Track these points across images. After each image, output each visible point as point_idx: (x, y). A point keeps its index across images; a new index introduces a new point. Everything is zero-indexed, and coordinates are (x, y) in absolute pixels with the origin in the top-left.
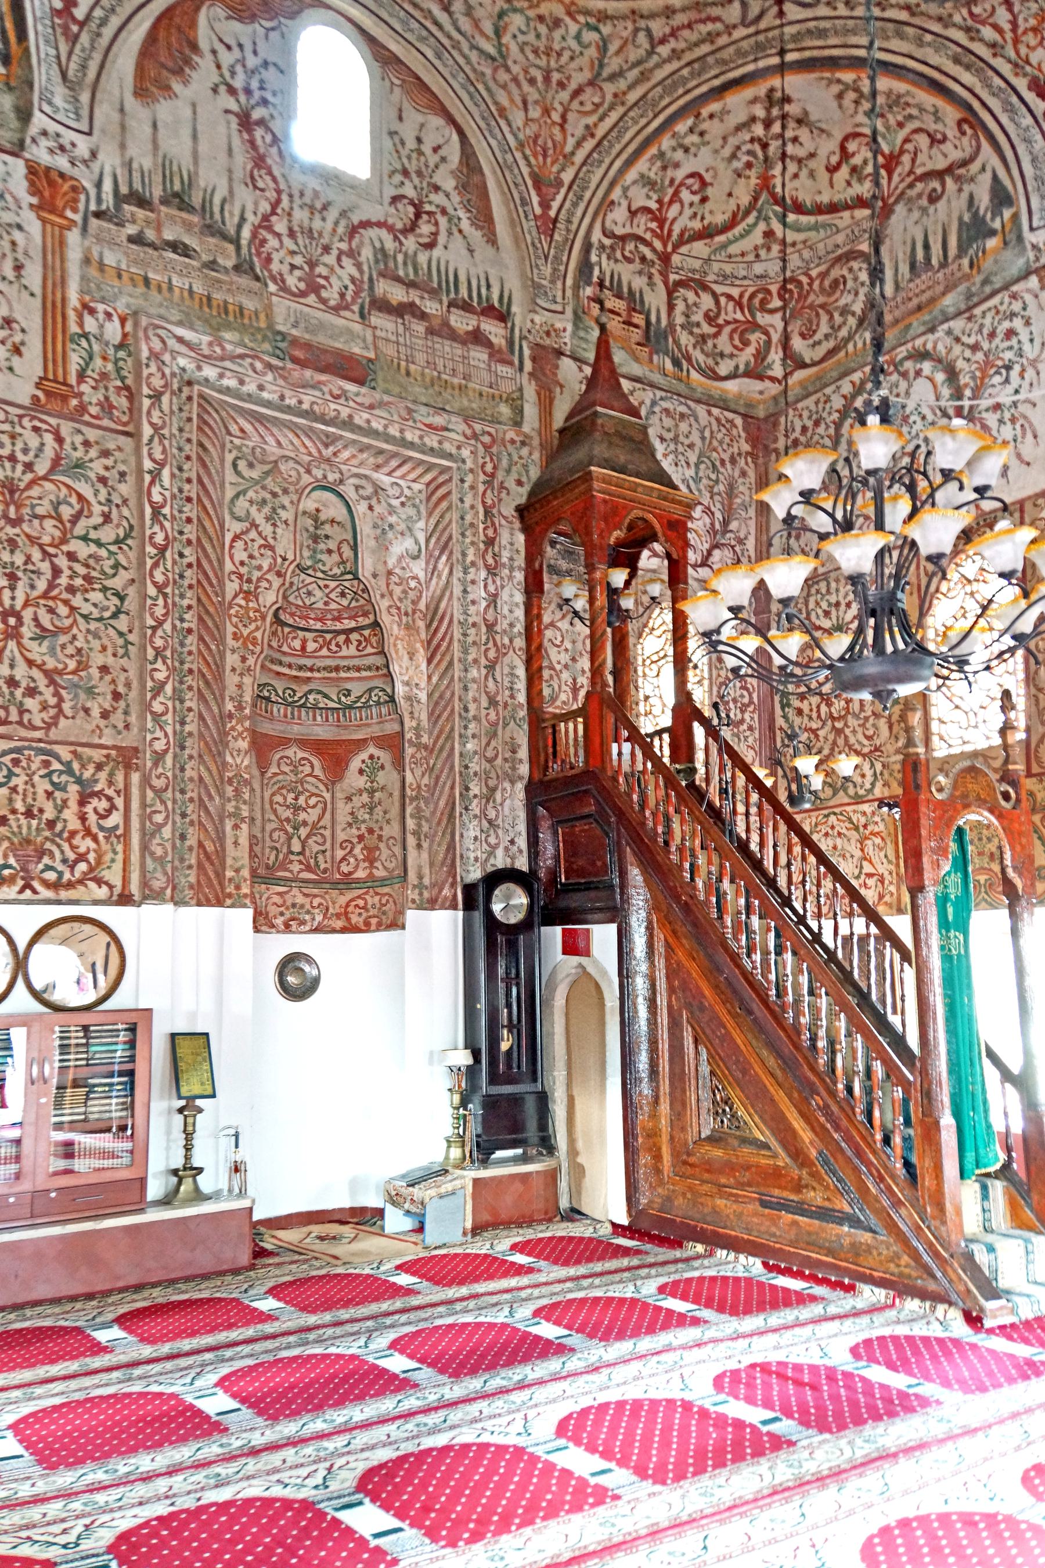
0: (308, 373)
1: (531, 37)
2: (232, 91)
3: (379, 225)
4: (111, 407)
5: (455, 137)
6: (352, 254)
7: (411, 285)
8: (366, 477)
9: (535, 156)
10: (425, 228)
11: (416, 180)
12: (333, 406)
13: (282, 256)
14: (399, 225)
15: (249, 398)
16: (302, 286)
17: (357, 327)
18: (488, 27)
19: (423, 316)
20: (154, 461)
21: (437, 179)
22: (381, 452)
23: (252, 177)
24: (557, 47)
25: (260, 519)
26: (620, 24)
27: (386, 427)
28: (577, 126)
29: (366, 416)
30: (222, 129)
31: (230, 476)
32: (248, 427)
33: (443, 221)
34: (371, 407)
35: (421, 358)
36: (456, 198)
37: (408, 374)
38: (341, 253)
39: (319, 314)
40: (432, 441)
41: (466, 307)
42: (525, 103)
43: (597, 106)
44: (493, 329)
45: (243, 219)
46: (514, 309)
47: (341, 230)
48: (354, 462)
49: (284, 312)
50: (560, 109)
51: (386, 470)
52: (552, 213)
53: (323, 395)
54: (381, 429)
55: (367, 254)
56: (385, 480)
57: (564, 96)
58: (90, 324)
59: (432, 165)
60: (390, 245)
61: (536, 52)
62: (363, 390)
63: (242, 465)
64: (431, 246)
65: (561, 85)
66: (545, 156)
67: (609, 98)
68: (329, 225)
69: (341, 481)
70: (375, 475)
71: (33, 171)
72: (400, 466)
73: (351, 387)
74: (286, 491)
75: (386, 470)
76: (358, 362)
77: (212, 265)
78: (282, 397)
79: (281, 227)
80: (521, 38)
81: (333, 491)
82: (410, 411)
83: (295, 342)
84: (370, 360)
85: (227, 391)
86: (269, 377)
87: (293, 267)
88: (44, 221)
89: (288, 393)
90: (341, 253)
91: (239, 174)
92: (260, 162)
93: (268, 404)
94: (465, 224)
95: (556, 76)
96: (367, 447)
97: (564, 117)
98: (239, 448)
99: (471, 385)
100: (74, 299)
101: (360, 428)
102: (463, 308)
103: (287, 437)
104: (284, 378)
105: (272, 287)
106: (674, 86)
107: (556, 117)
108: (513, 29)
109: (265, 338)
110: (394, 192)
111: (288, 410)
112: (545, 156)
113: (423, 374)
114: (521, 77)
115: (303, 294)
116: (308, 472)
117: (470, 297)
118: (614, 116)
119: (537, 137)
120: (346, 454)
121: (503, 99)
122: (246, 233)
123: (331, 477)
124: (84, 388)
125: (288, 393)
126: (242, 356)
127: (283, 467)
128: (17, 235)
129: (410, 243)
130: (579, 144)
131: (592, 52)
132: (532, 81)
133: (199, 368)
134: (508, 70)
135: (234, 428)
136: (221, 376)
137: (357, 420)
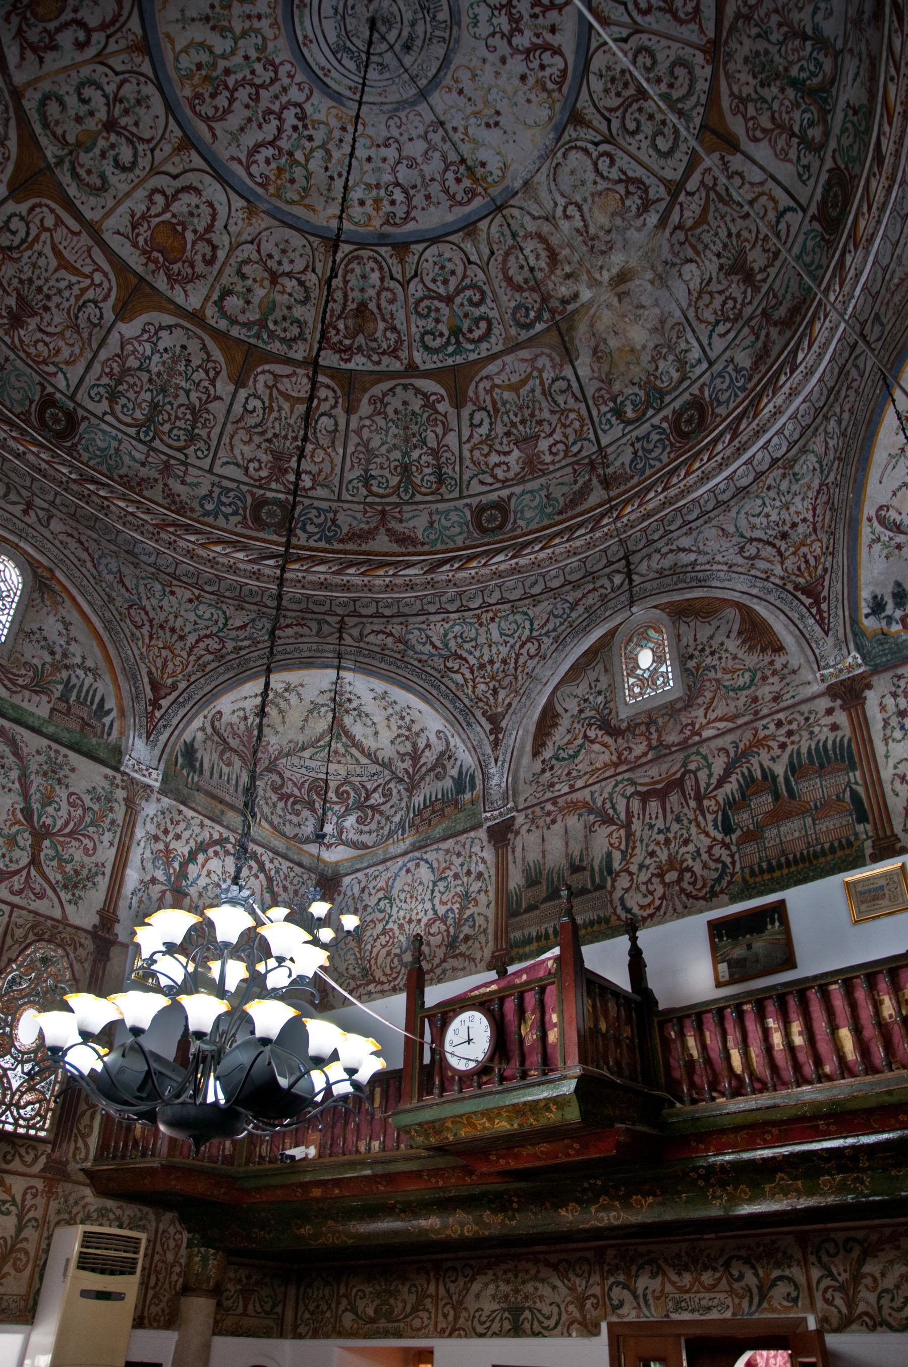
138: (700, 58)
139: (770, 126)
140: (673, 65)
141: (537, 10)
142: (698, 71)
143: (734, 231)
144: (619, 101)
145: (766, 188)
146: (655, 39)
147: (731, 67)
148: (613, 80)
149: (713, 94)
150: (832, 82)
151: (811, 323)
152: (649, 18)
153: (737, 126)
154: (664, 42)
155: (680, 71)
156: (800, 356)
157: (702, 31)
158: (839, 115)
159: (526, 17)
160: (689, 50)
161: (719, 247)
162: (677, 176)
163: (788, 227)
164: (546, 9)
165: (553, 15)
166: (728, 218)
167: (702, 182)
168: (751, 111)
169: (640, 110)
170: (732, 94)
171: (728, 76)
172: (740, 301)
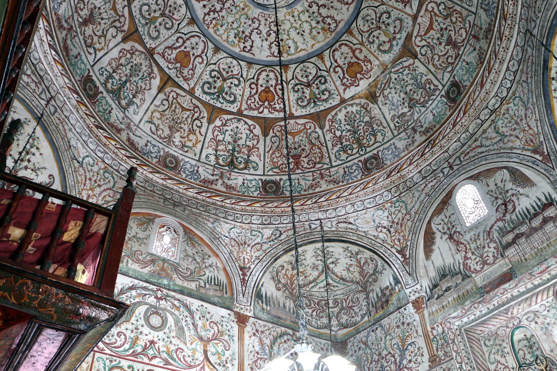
0: (491, 294)
1: (506, 121)
2: (445, 233)
3: (496, 222)
4: (447, 353)
5: (505, 170)
6: (491, 241)
7: (514, 228)
8: (528, 312)
9: (530, 145)
10: (510, 207)
11: (500, 197)
12: (504, 297)
13: (472, 264)
14: (502, 215)
15: (480, 317)
16: (481, 266)
17: (502, 262)
18: (494, 135)
19: (522, 234)
20: (459, 363)
21: (506, 189)
22: (527, 299)
23: (458, 249)
24: (513, 114)
25: (499, 358)
26: (518, 89)
27: (526, 287)
28: (533, 124)
29: (516, 290)
30: (447, 246)
31: (485, 349)
32: (481, 328)
33: (514, 198)
34: (516, 285)
35: (528, 250)
36: (514, 187)
37: (526, 260)
38: (488, 244)
39: (489, 270)
40: (546, 276)
41: (536, 215)
42: (517, 137)
43: (532, 113)
44: (550, 212)
45: (459, 264)
46: (553, 197)
47: (485, 237)
48: (521, 310)
49: (479, 280)
50: (526, 125)
51: (534, 303)
52: (546, 153)
53: (499, 296)
54: (524, 289)
55: (496, 235)
56: (535, 307)
57: (524, 121)
58: (435, 332)
59: (502, 187)
60: (500, 224)
61: (510, 122)
62: (511, 282)
63: (487, 342)
64: (514, 210)
65: (521, 120)
66: (532, 141)
67: (532, 107)
68: (482, 239)
69: (520, 321)
70: (531, 309)
71: (413, 303)
72: (537, 298)
73: (506, 286)
74: (503, 341)
75: (534, 303)
76: (507, 273)
77: (457, 285)
78: (488, 309)
79: (469, 255)
80: (504, 125)
81: (520, 327)
82: (530, 274)
83: (485, 286)
84: (511, 268)
85: (473, 321)
86: (481, 305)
87: (477, 263)
88: (418, 314)
89: (488, 306)
90: (488, 244)
91: (454, 252)
92: (458, 243)
93: (486, 314)
94: (522, 191)
95: (518, 120)
96: (521, 302)
97: (529, 126)
98: (484, 337)
99: (551, 240)
100: (429, 329)
101: (517, 296)
102: (535, 217)
103: (494, 322)
104: (485, 302)
105: (473, 275)
106: (537, 85)
107: (527, 129)
108: (501, 125)
109: (476, 293)
110: (495, 208)
111: (493, 310)
112: (532, 141)
113: (531, 255)
114: (511, 133)
115: (482, 268)
116: (508, 327)
117: (535, 210)
118: (536, 110)
119: (526, 140)
120: (515, 311)
121: (510, 145)
122: (462, 267)
123: (516, 324)
124: (439, 353)
125: (488, 306)
126: (471, 307)
127: (499, 333)
128: (415, 323)
129: (508, 217)
130: (537, 127)
131: (520, 103)
132: (515, 129)
133: (462, 321)
134: (506, 136)
135: (479, 332)
136: (469, 318)
137: (515, 294)
138: (153, 46)
139: (121, 62)
140: (159, 34)
141: (213, 8)
142: (151, 41)
143: (103, 22)
144: (169, 4)
145: (106, 48)
146: (170, 34)
147: (143, 56)
148: (175, 8)
149: (141, 42)
150: (119, 103)
151: (63, 66)
152: (176, 38)
153: (127, 46)
154: (167, 36)
155: (155, 34)
156: (53, 53)
157: (158, 53)
158: (111, 102)
159: (216, 4)
160: (158, 43)
161: (102, 11)
162: (132, 6)
163: (90, 54)
164: (210, 11)
165: (206, 10)
166: (107, 21)
167: (123, 16)
168: (129, 56)
169: (160, 9)
170: (137, 50)
171: (142, 53)
172: (81, 13)
